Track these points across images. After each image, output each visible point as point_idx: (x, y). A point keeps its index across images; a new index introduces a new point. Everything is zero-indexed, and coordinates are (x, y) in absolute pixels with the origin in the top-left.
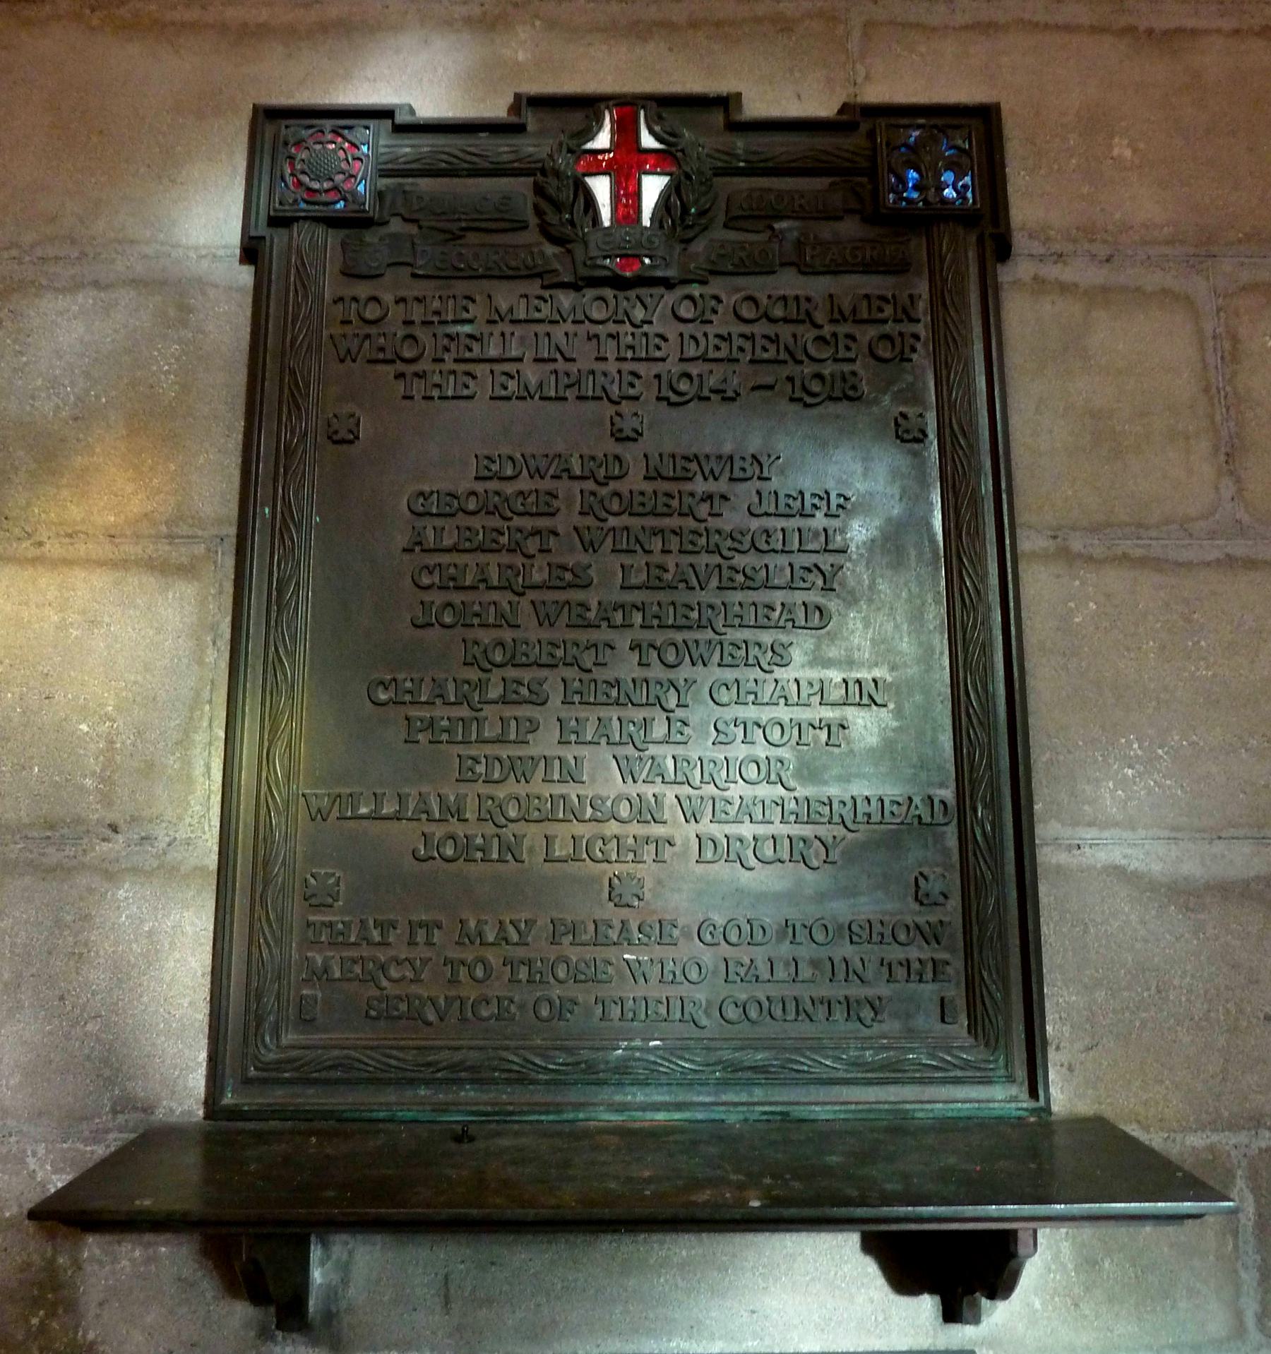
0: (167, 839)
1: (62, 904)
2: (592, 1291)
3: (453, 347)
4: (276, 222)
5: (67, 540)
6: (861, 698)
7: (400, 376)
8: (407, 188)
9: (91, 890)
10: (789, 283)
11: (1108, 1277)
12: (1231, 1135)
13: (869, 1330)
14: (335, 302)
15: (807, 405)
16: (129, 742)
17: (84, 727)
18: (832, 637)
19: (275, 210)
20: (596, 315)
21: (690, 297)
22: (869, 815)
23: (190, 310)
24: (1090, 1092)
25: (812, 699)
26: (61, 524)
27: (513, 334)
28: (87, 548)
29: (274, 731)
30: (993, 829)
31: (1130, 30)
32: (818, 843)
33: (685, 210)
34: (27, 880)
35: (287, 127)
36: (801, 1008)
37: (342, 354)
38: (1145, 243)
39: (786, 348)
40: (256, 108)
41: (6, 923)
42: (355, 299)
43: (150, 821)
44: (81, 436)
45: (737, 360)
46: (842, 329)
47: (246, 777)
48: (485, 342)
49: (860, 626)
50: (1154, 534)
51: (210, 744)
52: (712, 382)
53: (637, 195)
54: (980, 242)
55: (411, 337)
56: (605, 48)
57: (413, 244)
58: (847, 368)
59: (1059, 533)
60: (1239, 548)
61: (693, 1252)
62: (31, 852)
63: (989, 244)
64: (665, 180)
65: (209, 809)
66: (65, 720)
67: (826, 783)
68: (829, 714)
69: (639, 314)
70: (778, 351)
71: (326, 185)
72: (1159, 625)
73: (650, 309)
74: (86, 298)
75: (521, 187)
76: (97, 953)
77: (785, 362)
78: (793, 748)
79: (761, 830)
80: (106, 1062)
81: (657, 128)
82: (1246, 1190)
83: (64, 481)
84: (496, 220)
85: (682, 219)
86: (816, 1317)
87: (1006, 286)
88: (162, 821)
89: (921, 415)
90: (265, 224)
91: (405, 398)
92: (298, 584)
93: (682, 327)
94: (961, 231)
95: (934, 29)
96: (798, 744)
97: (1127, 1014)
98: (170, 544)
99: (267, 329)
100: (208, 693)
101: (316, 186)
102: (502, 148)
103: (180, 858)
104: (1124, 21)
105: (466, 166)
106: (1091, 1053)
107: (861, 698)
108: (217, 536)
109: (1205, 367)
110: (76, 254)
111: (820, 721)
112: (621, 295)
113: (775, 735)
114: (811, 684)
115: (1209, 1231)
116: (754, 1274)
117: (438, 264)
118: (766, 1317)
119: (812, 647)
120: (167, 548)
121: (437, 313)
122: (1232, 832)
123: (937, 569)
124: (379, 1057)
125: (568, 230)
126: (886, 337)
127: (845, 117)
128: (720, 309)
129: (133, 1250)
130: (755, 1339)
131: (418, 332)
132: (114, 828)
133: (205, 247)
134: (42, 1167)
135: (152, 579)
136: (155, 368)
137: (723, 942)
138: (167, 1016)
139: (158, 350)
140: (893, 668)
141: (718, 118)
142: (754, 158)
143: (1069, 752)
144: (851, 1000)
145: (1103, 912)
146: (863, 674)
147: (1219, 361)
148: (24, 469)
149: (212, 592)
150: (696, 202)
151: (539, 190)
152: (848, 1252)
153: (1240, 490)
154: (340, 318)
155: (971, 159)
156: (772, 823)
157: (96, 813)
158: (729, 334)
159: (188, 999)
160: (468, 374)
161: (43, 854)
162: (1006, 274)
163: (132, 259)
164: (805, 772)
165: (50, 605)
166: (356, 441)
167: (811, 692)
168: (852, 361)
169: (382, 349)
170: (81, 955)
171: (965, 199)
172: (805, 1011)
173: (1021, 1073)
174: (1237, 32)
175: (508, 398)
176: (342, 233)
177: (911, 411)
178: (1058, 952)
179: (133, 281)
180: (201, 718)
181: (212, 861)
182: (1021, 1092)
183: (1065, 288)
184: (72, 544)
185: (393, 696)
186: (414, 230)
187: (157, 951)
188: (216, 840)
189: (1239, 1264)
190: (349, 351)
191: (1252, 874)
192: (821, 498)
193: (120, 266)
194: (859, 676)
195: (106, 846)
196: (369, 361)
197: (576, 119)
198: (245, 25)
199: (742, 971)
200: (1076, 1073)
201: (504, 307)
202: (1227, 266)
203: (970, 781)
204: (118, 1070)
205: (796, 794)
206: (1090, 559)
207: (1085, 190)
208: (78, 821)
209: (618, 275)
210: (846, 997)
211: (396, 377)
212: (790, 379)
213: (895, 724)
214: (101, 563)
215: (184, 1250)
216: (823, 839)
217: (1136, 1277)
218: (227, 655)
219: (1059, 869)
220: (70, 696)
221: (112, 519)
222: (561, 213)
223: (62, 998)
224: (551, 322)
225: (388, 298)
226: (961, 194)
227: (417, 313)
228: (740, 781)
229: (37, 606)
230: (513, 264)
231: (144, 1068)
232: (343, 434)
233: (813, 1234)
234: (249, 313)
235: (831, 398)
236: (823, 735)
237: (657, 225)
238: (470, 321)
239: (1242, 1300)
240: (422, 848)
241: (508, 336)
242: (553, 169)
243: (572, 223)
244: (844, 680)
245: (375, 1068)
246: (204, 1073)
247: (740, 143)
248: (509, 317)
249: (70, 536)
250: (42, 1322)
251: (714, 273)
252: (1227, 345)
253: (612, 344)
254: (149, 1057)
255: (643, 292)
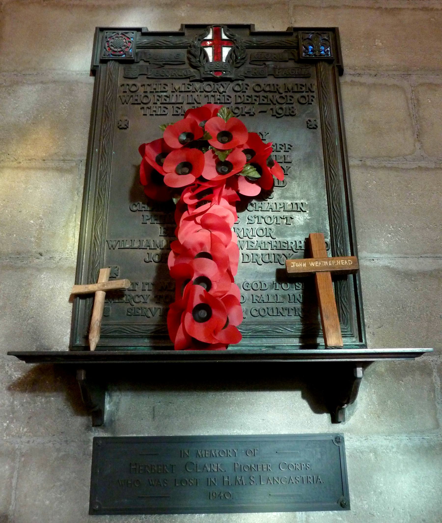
0: (59, 258)
1: (21, 280)
2: (206, 413)
3: (160, 99)
4: (104, 61)
5: (29, 161)
6: (297, 209)
7: (142, 108)
8: (145, 52)
9: (32, 275)
10: (271, 80)
11: (390, 407)
12: (430, 357)
13: (305, 426)
14: (121, 86)
15: (278, 117)
16: (47, 226)
17: (32, 222)
18: (287, 190)
19: (102, 57)
20: (207, 90)
21: (238, 85)
22: (300, 247)
23: (73, 90)
24: (381, 342)
25: (281, 209)
26: (27, 156)
27: (180, 95)
28: (36, 164)
29: (97, 220)
30: (344, 251)
31: (379, 8)
32: (283, 256)
33: (236, 57)
34: (10, 271)
35: (107, 33)
36: (279, 311)
37: (123, 102)
38: (387, 70)
39: (270, 100)
40: (96, 28)
41: (2, 286)
42: (128, 85)
43: (53, 252)
44: (35, 129)
45: (254, 104)
46: (289, 94)
47: (87, 235)
48: (171, 97)
49: (296, 186)
50: (394, 159)
51: (75, 226)
52: (246, 110)
53: (221, 53)
54: (334, 68)
55: (146, 96)
56: (210, 12)
57: (147, 68)
58: (290, 106)
59: (363, 159)
60: (423, 164)
61: (242, 399)
62: (12, 262)
63: (336, 69)
64: (230, 49)
65: (74, 248)
66: (26, 219)
67: (286, 237)
68: (286, 214)
69: (222, 90)
70: (268, 100)
71: (119, 50)
72: (397, 188)
73: (225, 88)
74: (38, 87)
75: (183, 52)
76: (33, 296)
77: (270, 104)
78: (274, 225)
79: (264, 252)
80: (35, 333)
81: (227, 33)
82: (437, 376)
83: (29, 143)
84: (175, 61)
85: (236, 61)
86: (286, 422)
87: (342, 84)
88: (58, 252)
89: (315, 121)
90: (99, 62)
91: (144, 115)
92: (107, 173)
93: (235, 94)
94: (326, 64)
95: (317, 8)
96: (276, 224)
97: (392, 316)
98: (63, 162)
99: (98, 94)
100: (75, 210)
101: (116, 50)
102: (176, 40)
103: (63, 263)
104: (377, 5)
105: (165, 45)
106: (380, 329)
107: (297, 209)
108: (80, 160)
109: (408, 108)
110: (36, 73)
111: (284, 216)
112: (216, 84)
113: (268, 221)
114: (280, 204)
115: (425, 391)
116: (264, 406)
117: (155, 74)
118: (268, 421)
119: (280, 193)
120: (63, 163)
121: (155, 89)
122: (426, 255)
123: (325, 190)
124: (132, 328)
125: (198, 64)
126: (303, 97)
127: (288, 32)
128: (248, 88)
129: (42, 399)
130: (264, 430)
131: (148, 94)
132: (41, 255)
133: (78, 71)
134: (10, 369)
135: (57, 174)
136: (60, 108)
137: (251, 289)
138: (57, 317)
139: (62, 102)
140: (308, 200)
141: (247, 32)
142: (259, 43)
143: (369, 229)
144: (296, 308)
145: (382, 281)
146: (298, 202)
147: (413, 106)
148: (15, 139)
149: (78, 178)
150: (240, 55)
151: (189, 52)
152: (297, 398)
153: (422, 146)
154: (123, 91)
155: (330, 43)
156: (268, 249)
157: (34, 249)
158: (251, 95)
159: (65, 311)
160: (165, 107)
161: (15, 263)
162: (342, 80)
163: (54, 75)
164: (279, 233)
165: (22, 182)
166: (127, 129)
167: (281, 207)
168: (292, 104)
169: (137, 100)
170: (28, 296)
171: (328, 54)
172: (280, 312)
173: (356, 333)
174: (413, 9)
175: (178, 115)
176: (124, 65)
177: (312, 119)
178: (368, 295)
179: (54, 81)
180: (72, 218)
181: (74, 265)
182: (357, 340)
183: (361, 84)
184: (30, 163)
185: (138, 208)
186: (147, 64)
187: (54, 295)
188: (76, 258)
189: (436, 403)
190: (125, 101)
191: (433, 268)
192: (283, 146)
193: (50, 77)
194: (296, 202)
195: (38, 260)
196: (132, 104)
197: (201, 31)
198: (94, 6)
199: (258, 299)
200: (375, 336)
201: (177, 88)
202: (414, 77)
203: (335, 235)
204: (39, 336)
205: (276, 240)
206: (373, 168)
207: (367, 55)
208: (29, 252)
209: (215, 77)
210: (294, 308)
211: (141, 109)
212: (272, 109)
213: (309, 218)
214: (40, 169)
215: (60, 399)
216: (285, 254)
217: (400, 407)
218: (82, 198)
219: (367, 267)
220: (27, 211)
221: (44, 154)
222: (196, 58)
223: (20, 311)
224: (193, 92)
225: (139, 84)
226: (326, 53)
227: (149, 89)
228: (257, 236)
229: (18, 182)
230: (180, 74)
231: (48, 335)
232: (123, 126)
233: (285, 392)
234: (92, 91)
235: (286, 115)
236: (285, 221)
237: (227, 62)
238: (166, 92)
239: (438, 415)
240: (147, 258)
241: (178, 96)
242: (193, 45)
243: (200, 61)
244: (292, 204)
245: (130, 332)
246: (69, 337)
247: (254, 39)
248: (179, 90)
249: (29, 160)
250: (8, 425)
251: (246, 77)
252: (416, 102)
253: (212, 99)
254: (50, 331)
255: (222, 83)
